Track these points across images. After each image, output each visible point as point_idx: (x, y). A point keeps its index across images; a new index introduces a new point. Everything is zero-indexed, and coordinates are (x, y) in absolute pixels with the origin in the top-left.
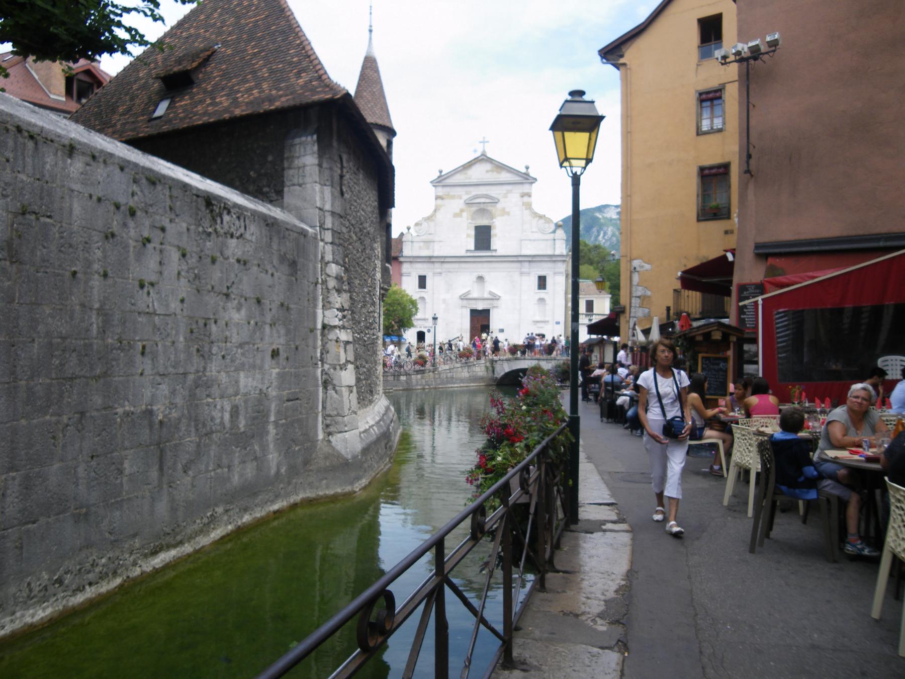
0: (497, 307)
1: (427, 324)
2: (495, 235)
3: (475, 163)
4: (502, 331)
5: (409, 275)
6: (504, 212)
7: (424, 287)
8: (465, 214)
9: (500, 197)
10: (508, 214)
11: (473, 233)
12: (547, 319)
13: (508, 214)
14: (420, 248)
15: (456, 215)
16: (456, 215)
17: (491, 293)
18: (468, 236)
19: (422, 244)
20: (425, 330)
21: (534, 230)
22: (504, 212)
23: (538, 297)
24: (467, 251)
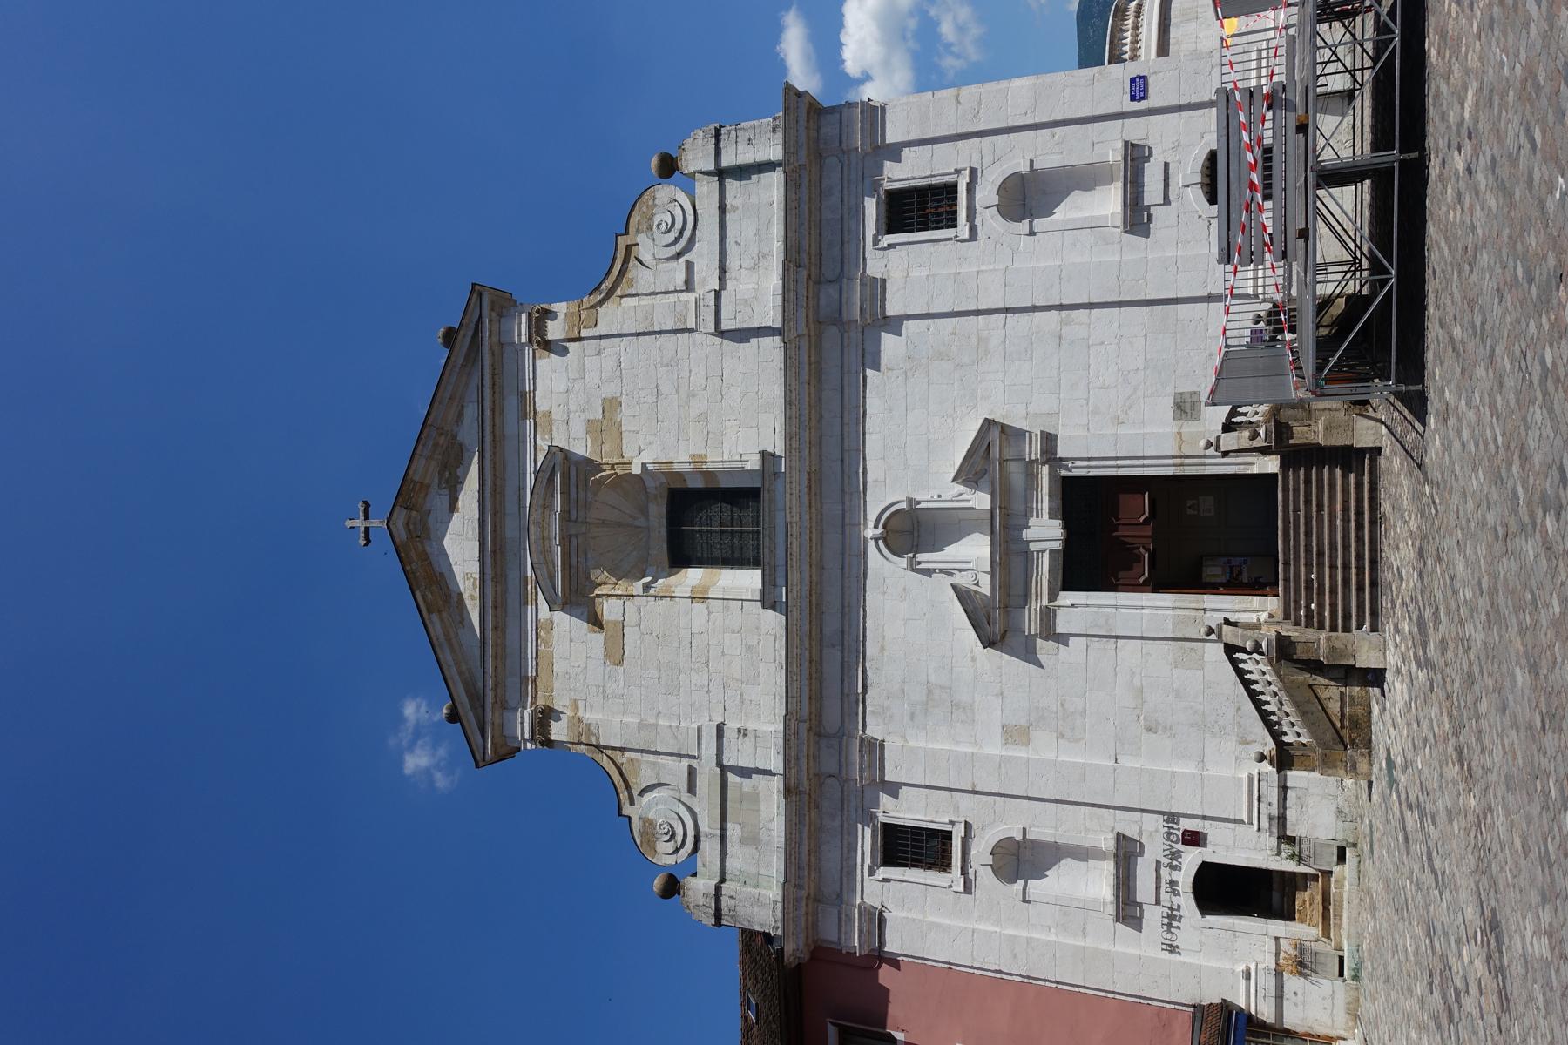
0: (1049, 440)
1: (1155, 849)
2: (698, 461)
3: (425, 557)
4: (1184, 408)
5: (877, 920)
6: (606, 424)
7: (946, 836)
8: (610, 610)
9: (543, 445)
10: (611, 405)
11: (693, 576)
12: (1114, 155)
13: (611, 405)
14: (751, 839)
15: (615, 654)
16: (615, 654)
17: (970, 473)
18: (698, 597)
19: (733, 830)
20: (1192, 859)
21: (680, 278)
22: (606, 424)
23: (990, 221)
24: (768, 599)
